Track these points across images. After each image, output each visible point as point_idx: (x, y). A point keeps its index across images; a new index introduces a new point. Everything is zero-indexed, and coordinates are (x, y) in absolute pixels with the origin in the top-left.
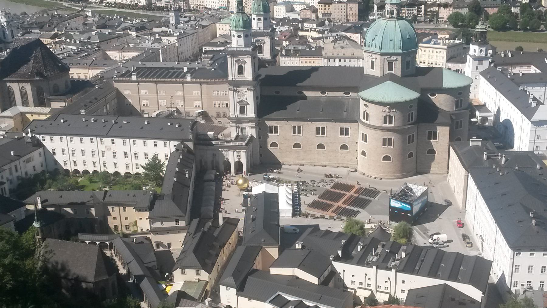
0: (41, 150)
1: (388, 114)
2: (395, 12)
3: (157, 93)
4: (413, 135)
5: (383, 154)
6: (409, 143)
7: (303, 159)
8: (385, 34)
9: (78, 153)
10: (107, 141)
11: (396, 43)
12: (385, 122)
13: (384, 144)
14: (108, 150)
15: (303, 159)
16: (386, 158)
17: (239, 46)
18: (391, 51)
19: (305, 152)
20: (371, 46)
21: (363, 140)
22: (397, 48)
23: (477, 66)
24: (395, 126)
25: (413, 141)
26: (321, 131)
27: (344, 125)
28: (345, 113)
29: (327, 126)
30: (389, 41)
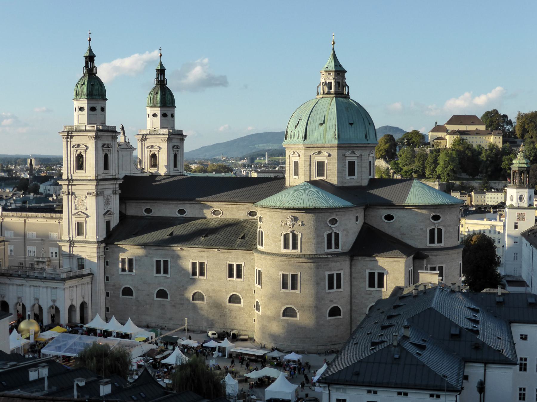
1: (289, 231)
2: (333, 84)
4: (339, 276)
5: (284, 304)
6: (331, 287)
7: (171, 319)
8: (312, 114)
11: (328, 129)
12: (286, 246)
15: (171, 319)
17: (80, 125)
18: (321, 142)
19: (174, 306)
20: (292, 137)
21: (256, 283)
22: (330, 137)
23: (516, 222)
24: (303, 253)
25: (339, 286)
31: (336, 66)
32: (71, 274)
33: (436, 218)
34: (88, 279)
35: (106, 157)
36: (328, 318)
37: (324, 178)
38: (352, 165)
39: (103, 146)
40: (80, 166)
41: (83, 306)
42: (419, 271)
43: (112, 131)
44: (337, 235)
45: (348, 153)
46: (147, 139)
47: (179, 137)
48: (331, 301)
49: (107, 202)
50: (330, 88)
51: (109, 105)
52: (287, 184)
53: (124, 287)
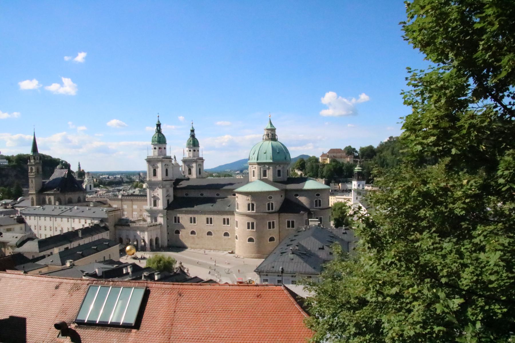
0: (23, 225)
2: (270, 135)
3: (132, 207)
4: (273, 222)
6: (270, 228)
8: (261, 149)
9: (43, 228)
10: (59, 219)
12: (249, 210)
13: (249, 228)
14: (59, 226)
16: (250, 240)
25: (273, 227)
26: (209, 221)
27: (226, 217)
28: (228, 207)
29: (214, 217)
30: (263, 153)
31: (271, 126)
32: (152, 224)
33: (318, 195)
34: (159, 226)
35: (167, 170)
36: (269, 242)
37: (267, 178)
38: (279, 171)
39: (165, 165)
40: (155, 174)
41: (157, 239)
42: (309, 220)
43: (170, 158)
44: (272, 204)
45: (277, 166)
46: (82, 169)
47: (201, 160)
48: (270, 234)
49: (167, 191)
50: (269, 136)
51: (168, 147)
52: (250, 181)
53: (175, 230)
